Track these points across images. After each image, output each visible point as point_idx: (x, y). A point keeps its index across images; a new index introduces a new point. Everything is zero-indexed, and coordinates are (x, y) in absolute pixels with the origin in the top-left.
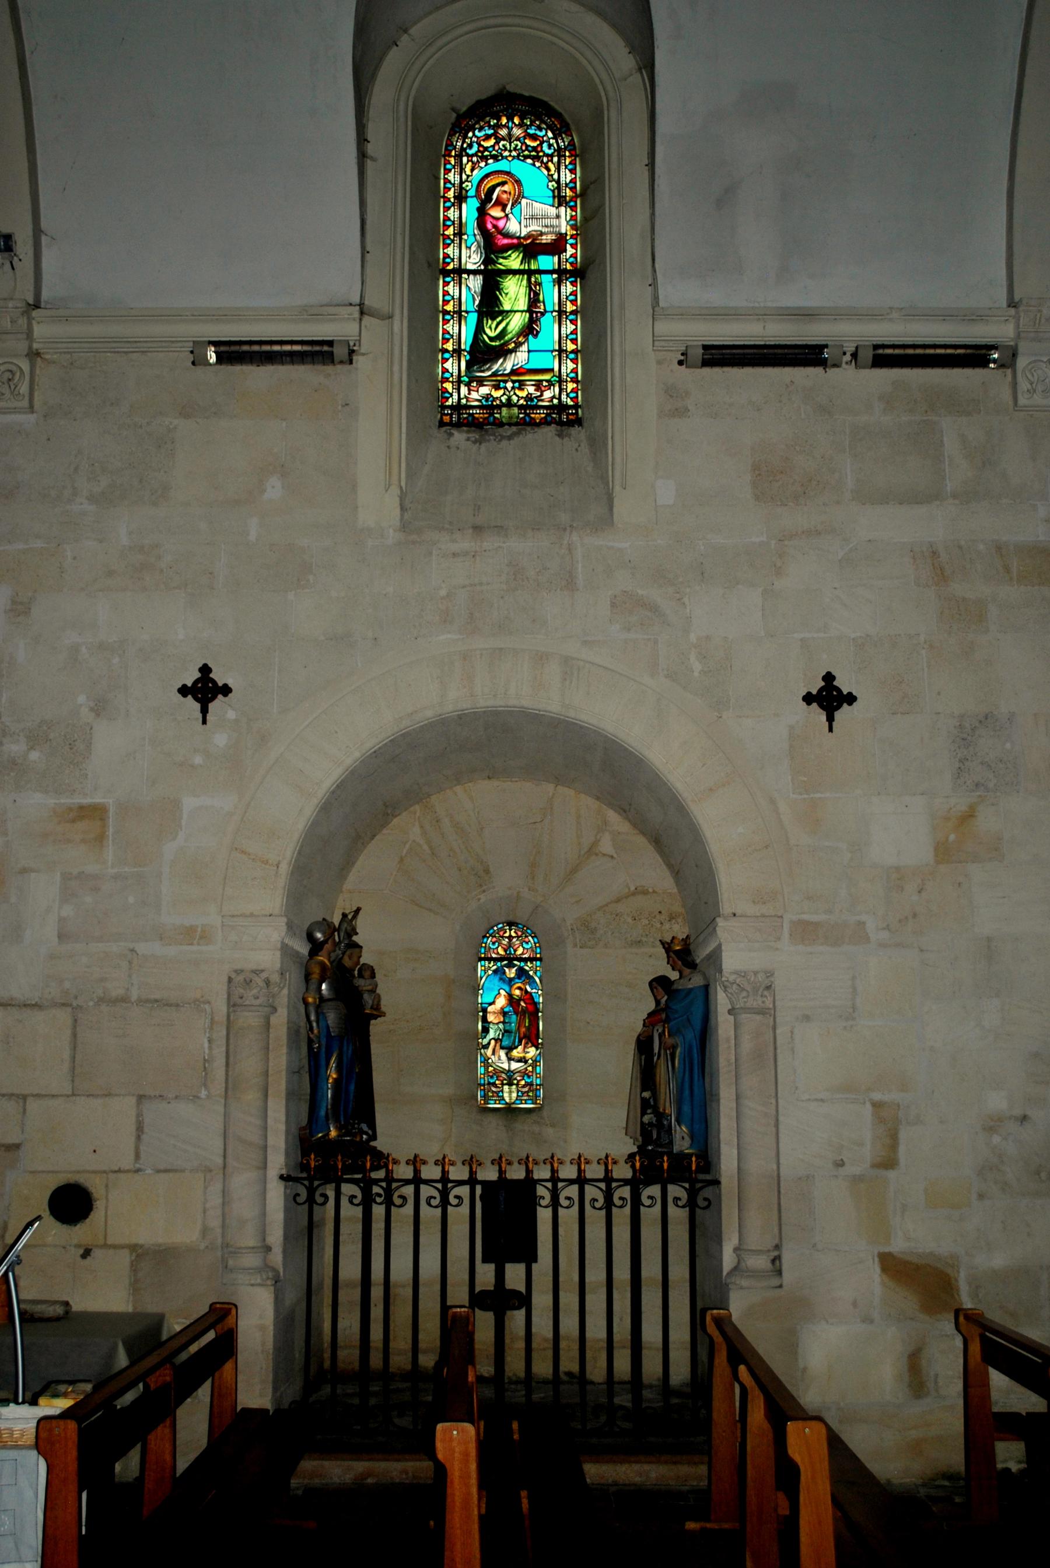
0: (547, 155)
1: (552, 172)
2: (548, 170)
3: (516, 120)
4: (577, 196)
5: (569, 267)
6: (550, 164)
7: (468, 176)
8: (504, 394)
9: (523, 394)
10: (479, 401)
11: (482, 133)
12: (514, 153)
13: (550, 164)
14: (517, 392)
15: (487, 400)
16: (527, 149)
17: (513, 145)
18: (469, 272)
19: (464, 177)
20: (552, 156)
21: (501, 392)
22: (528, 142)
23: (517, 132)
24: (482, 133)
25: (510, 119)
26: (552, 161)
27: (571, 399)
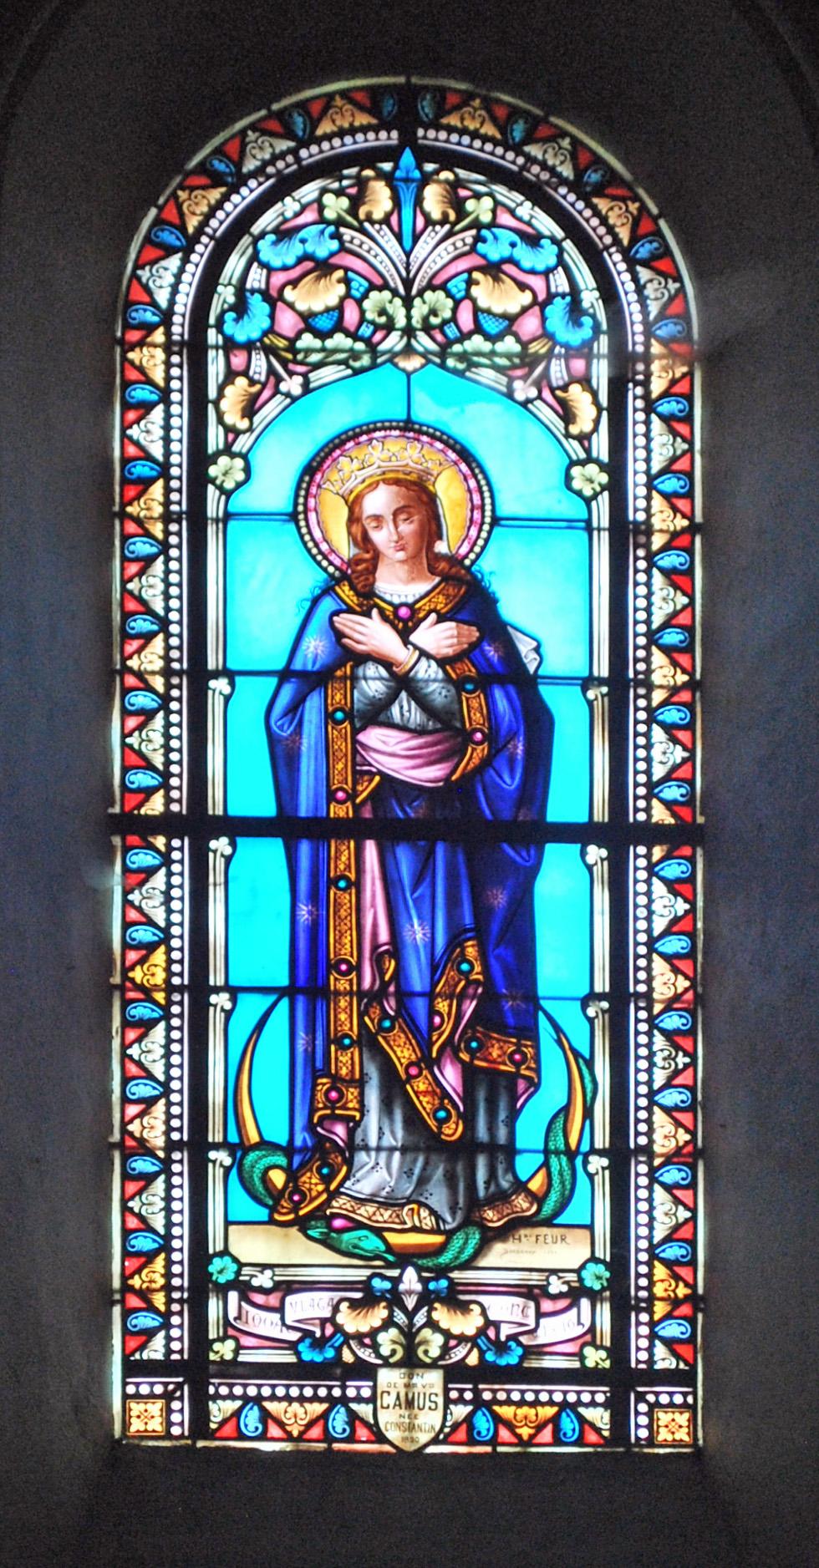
0: (571, 352)
1: (583, 424)
2: (567, 415)
3: (433, 200)
4: (693, 529)
5: (660, 814)
6: (576, 393)
7: (232, 432)
8: (388, 1323)
9: (467, 1324)
10: (292, 1346)
11: (289, 253)
12: (423, 341)
13: (576, 393)
14: (441, 1315)
15: (319, 1344)
16: (478, 329)
17: (419, 310)
18: (241, 828)
19: (215, 438)
20: (585, 351)
21: (380, 1313)
22: (486, 293)
23: (434, 254)
24: (289, 253)
25: (407, 191)
26: (586, 382)
27: (669, 1343)
